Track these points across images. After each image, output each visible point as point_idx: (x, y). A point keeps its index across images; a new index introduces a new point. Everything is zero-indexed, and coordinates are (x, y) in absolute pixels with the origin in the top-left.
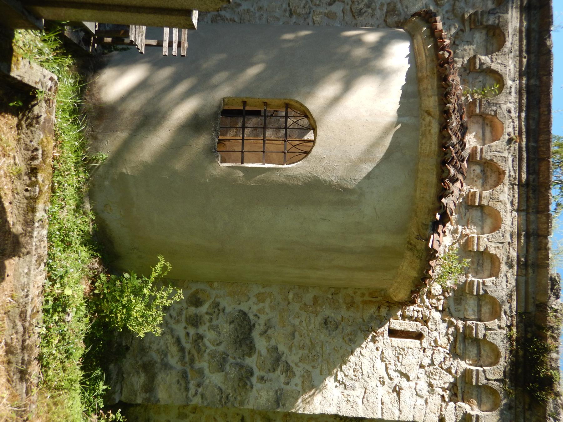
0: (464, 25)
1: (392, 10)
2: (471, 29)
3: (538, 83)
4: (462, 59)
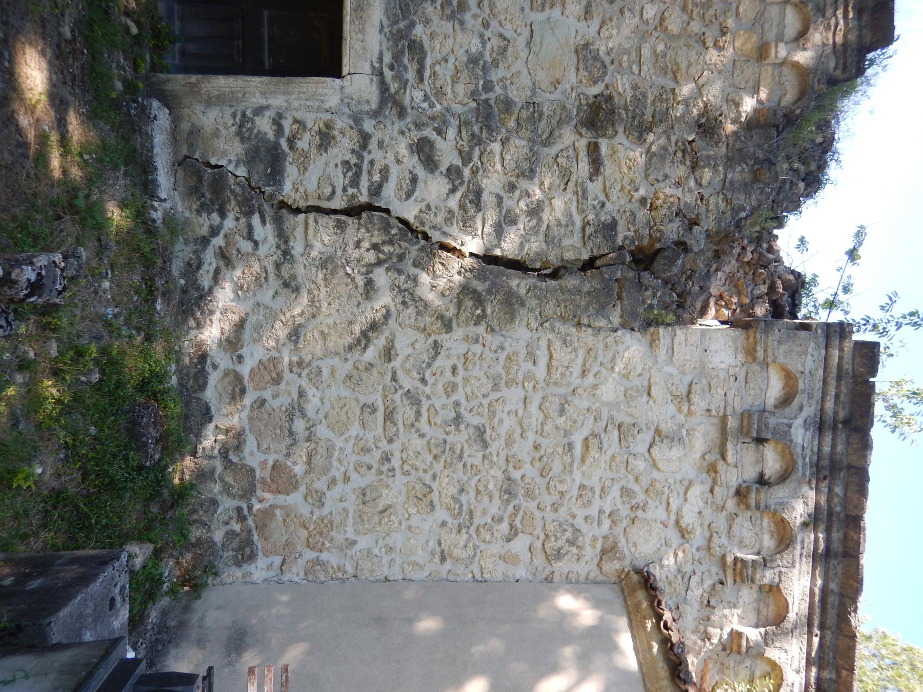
0: (725, 571)
1: (609, 551)
2: (735, 581)
3: (834, 676)
4: (718, 631)
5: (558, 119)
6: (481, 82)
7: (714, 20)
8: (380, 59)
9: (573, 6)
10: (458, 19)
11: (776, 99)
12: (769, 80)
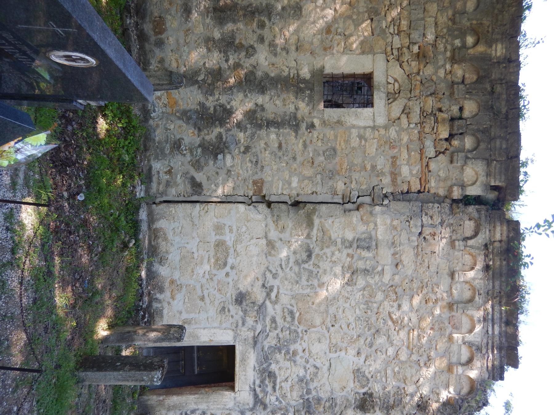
5: (345, 405)
6: (305, 390)
7: (424, 353)
8: (254, 383)
9: (351, 351)
10: (293, 360)
11: (458, 390)
12: (454, 381)
